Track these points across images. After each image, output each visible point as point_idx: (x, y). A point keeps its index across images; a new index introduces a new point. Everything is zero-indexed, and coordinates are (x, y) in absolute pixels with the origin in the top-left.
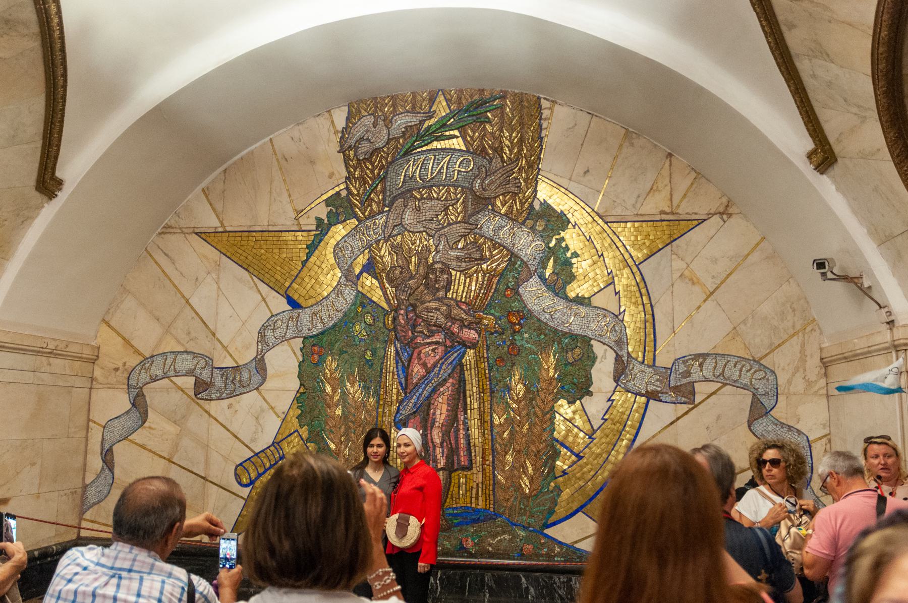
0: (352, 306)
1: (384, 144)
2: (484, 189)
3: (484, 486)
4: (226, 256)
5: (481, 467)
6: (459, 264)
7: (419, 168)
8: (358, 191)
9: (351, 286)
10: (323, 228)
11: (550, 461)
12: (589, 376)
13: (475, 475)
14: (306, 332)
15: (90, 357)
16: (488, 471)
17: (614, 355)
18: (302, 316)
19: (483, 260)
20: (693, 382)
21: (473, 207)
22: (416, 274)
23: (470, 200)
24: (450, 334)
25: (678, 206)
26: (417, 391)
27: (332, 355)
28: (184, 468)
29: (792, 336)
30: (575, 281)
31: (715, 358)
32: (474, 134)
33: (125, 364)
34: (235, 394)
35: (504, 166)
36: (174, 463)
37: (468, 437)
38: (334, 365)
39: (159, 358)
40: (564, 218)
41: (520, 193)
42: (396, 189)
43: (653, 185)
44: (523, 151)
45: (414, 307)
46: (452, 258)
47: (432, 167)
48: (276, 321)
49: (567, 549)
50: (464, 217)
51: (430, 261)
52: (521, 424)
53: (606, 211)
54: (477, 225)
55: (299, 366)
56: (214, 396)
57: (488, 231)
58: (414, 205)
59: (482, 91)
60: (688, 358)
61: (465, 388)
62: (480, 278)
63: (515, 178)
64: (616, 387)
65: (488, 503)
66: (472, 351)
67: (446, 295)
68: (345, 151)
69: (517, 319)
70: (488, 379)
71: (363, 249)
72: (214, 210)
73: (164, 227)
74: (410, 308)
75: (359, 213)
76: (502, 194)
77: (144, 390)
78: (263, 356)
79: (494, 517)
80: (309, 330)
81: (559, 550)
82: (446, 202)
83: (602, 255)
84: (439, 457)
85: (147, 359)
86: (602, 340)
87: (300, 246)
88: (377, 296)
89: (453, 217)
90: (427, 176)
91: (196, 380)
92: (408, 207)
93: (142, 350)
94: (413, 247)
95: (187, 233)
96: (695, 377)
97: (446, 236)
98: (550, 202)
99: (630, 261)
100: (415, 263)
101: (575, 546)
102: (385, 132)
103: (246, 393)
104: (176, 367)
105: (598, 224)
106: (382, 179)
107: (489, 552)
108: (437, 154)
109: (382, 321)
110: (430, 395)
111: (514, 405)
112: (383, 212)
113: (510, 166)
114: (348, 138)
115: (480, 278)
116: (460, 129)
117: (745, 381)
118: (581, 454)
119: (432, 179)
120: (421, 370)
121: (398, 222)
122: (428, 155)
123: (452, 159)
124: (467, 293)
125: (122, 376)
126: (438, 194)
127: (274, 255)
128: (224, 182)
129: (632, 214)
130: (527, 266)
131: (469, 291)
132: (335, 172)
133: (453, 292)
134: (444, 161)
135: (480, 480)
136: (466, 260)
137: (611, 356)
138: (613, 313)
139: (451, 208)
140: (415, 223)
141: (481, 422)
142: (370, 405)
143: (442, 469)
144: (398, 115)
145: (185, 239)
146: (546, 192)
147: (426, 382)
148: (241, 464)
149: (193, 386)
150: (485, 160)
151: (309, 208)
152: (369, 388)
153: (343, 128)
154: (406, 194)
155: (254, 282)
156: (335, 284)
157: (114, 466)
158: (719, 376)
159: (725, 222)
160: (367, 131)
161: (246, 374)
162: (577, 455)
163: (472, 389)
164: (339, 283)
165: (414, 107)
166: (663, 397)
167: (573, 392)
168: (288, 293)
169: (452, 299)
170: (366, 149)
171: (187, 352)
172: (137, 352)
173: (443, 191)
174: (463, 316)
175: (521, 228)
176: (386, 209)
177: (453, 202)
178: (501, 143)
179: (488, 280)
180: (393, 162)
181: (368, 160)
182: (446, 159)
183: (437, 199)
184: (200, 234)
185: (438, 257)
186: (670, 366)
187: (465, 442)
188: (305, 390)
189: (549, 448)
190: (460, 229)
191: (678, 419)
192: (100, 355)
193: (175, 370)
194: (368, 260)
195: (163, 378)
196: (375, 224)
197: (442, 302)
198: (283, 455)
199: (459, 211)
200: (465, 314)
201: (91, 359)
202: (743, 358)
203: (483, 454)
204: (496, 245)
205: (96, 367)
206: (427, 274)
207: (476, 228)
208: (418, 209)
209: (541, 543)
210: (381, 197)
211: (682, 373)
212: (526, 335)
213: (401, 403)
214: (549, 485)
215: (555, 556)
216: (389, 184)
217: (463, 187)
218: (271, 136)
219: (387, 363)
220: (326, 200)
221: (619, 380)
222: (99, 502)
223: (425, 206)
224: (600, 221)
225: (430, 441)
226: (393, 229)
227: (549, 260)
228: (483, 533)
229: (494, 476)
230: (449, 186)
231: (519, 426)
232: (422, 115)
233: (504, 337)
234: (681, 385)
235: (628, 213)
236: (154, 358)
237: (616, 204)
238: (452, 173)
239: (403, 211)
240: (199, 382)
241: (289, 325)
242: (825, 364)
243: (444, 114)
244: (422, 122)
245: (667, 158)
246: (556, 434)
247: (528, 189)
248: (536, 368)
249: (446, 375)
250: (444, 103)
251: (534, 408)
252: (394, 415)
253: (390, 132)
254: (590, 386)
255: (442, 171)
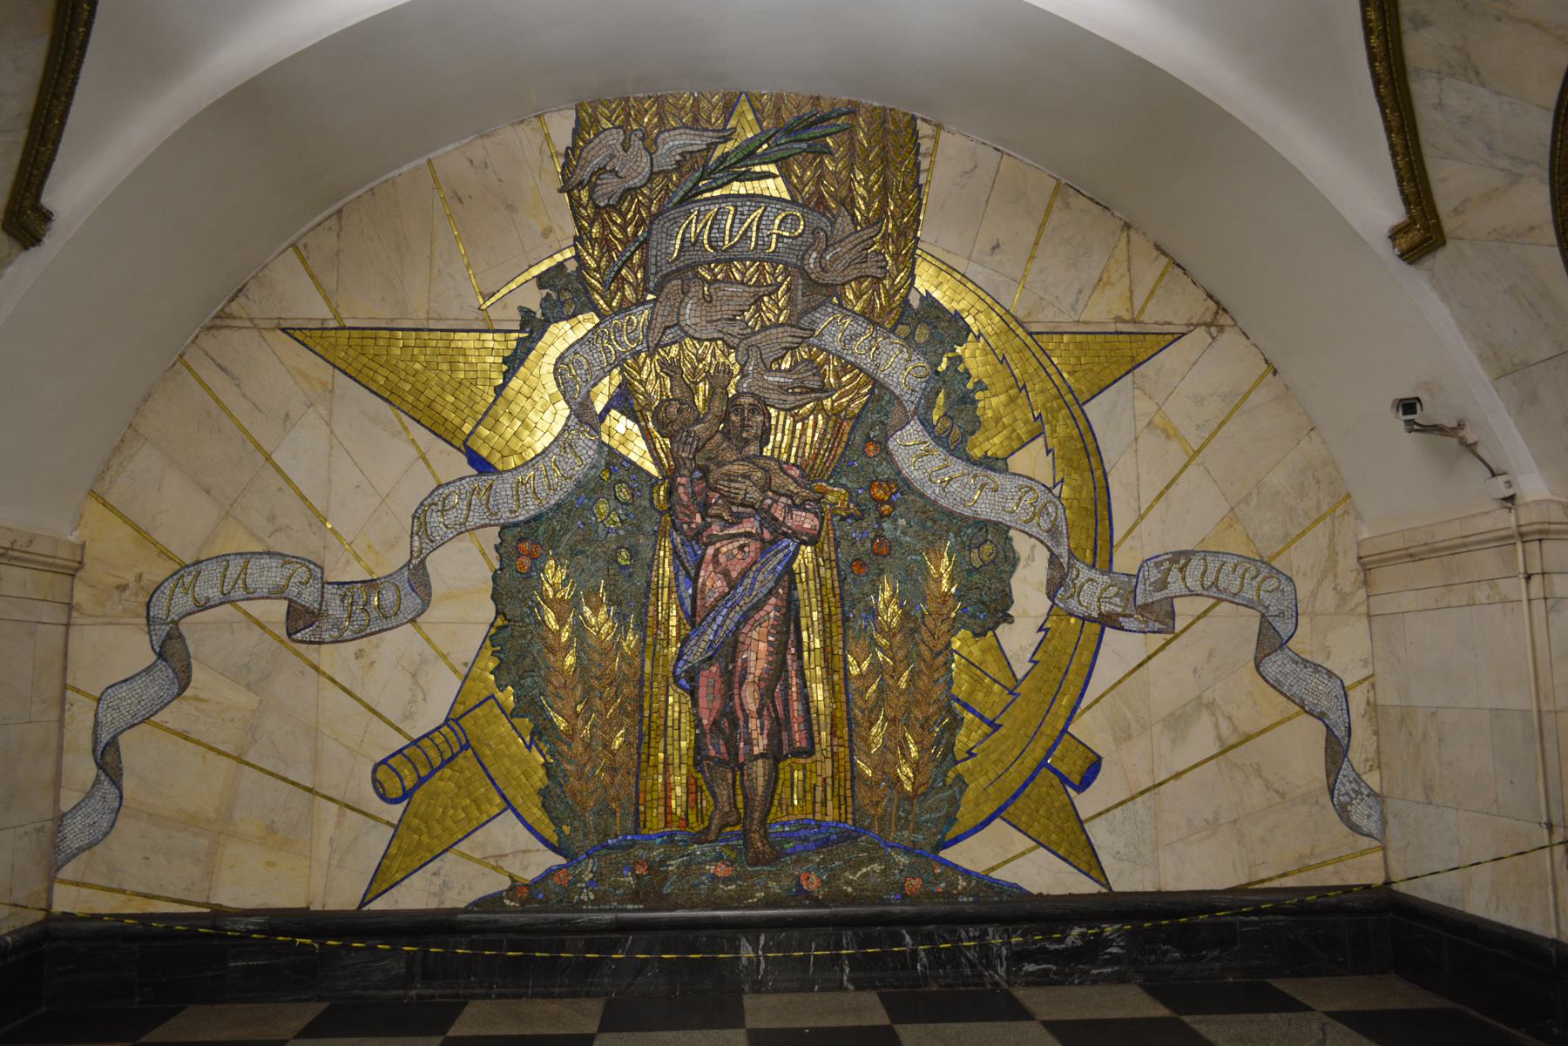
0: (591, 468)
1: (644, 181)
2: (823, 269)
3: (836, 782)
4: (346, 374)
5: (829, 749)
6: (784, 397)
7: (708, 227)
8: (598, 263)
9: (589, 433)
10: (533, 327)
11: (946, 735)
12: (1008, 591)
13: (819, 764)
14: (505, 516)
15: (69, 564)
16: (842, 756)
17: (1047, 554)
18: (498, 486)
19: (825, 392)
20: (1172, 598)
21: (806, 299)
22: (706, 414)
23: (800, 287)
24: (768, 519)
25: (1142, 310)
26: (714, 619)
27: (557, 557)
28: (271, 774)
29: (1317, 521)
30: (982, 429)
31: (1204, 559)
32: (804, 172)
33: (139, 578)
34: (368, 631)
35: (857, 232)
36: (248, 764)
37: (806, 698)
38: (561, 574)
39: (213, 566)
40: (961, 323)
41: (885, 278)
42: (668, 262)
43: (1102, 273)
44: (888, 206)
45: (705, 472)
46: (771, 387)
47: (732, 226)
48: (448, 496)
49: (978, 882)
50: (791, 315)
51: (732, 391)
52: (895, 674)
53: (1029, 314)
54: (814, 330)
55: (494, 578)
56: (326, 636)
57: (833, 342)
58: (701, 292)
59: (816, 100)
60: (1162, 558)
61: (798, 612)
62: (821, 422)
63: (877, 253)
64: (1052, 607)
65: (843, 811)
66: (809, 549)
67: (761, 451)
68: (572, 190)
69: (885, 494)
70: (838, 597)
71: (609, 368)
72: (319, 286)
73: (217, 317)
74: (698, 474)
75: (601, 302)
76: (855, 279)
77: (183, 627)
78: (423, 562)
79: (854, 834)
80: (511, 512)
81: (964, 884)
82: (757, 289)
83: (1024, 386)
84: (754, 735)
85: (187, 566)
86: (1026, 530)
87: (490, 359)
88: (637, 452)
89: (770, 316)
90: (724, 241)
91: (289, 606)
92: (690, 295)
93: (174, 548)
94: (701, 366)
95: (265, 329)
96: (1175, 587)
97: (759, 348)
98: (936, 294)
99: (1069, 397)
100: (704, 395)
101: (990, 875)
102: (645, 160)
103: (391, 629)
104: (249, 581)
105: (1017, 335)
106: (641, 243)
107: (847, 895)
108: (739, 204)
109: (647, 496)
110: (738, 625)
111: (884, 642)
112: (646, 302)
113: (867, 231)
114: (576, 166)
115: (821, 422)
116: (780, 163)
117: (1250, 594)
118: (997, 722)
119: (731, 247)
120: (719, 583)
121: (672, 320)
122: (723, 205)
123: (766, 214)
124: (798, 448)
125: (136, 602)
126: (743, 275)
127: (441, 375)
128: (338, 236)
129: (1071, 320)
130: (901, 403)
131: (802, 445)
132: (555, 227)
133: (774, 447)
134: (752, 217)
135: (829, 772)
136: (796, 390)
137: (1042, 555)
138: (1043, 485)
139: (766, 299)
140: (704, 323)
141: (827, 672)
142: (628, 646)
143: (762, 756)
144: (668, 130)
145: (260, 339)
146: (927, 280)
147: (730, 603)
148: (384, 762)
149: (284, 618)
150: (824, 219)
151: (504, 291)
152: (625, 617)
153: (568, 148)
154: (686, 271)
155: (400, 420)
156: (557, 429)
157: (121, 775)
158: (1211, 586)
159: (1213, 338)
160: (612, 157)
161: (390, 594)
162: (991, 723)
163: (812, 615)
164: (566, 428)
165: (696, 120)
166: (1126, 623)
167: (982, 616)
168: (469, 443)
169: (771, 458)
170: (610, 189)
171: (270, 554)
172: (165, 554)
173: (752, 269)
174: (792, 488)
175: (889, 337)
176: (650, 297)
177: (770, 289)
178: (851, 190)
179: (834, 427)
180: (660, 213)
181: (615, 208)
182: (755, 214)
183: (742, 283)
184: (291, 332)
185: (745, 385)
186: (1135, 573)
187: (800, 708)
188: (506, 623)
189: (944, 713)
190: (785, 336)
191: (1149, 658)
192: (86, 560)
193: (246, 587)
194: (619, 386)
195: (221, 604)
196: (630, 322)
197: (754, 463)
198: (468, 741)
199: (780, 304)
200: (795, 485)
201: (70, 568)
202: (1246, 558)
203: (832, 728)
204: (846, 367)
205: (78, 583)
206: (727, 413)
207: (812, 336)
208: (708, 300)
209: (934, 875)
210: (639, 276)
211: (1154, 582)
212: (902, 522)
213: (684, 641)
214: (945, 775)
215: (959, 894)
216: (654, 252)
217: (786, 265)
218: (431, 156)
219: (658, 570)
220: (539, 277)
221: (1055, 596)
222: (90, 846)
223: (720, 293)
224: (1019, 331)
225: (738, 707)
226: (663, 333)
227: (937, 394)
228: (837, 863)
229: (853, 764)
230: (762, 261)
231: (893, 677)
232: (711, 134)
233: (864, 524)
234: (1153, 603)
235: (1065, 318)
236: (203, 566)
237: (1045, 302)
238: (766, 239)
239: (681, 302)
240: (296, 609)
241: (474, 502)
242: (1366, 566)
243: (750, 135)
244: (711, 147)
245: (1122, 231)
246: (955, 691)
247: (899, 272)
248: (919, 578)
249: (765, 591)
250: (750, 117)
251: (917, 645)
252: (673, 663)
253: (655, 161)
254: (1008, 607)
255: (749, 234)
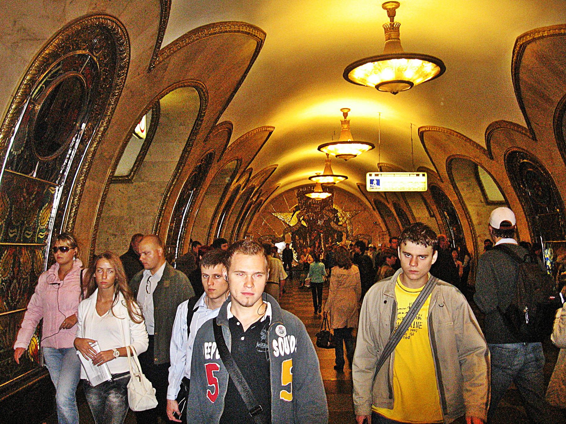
10: (294, 212)
146: (334, 206)
